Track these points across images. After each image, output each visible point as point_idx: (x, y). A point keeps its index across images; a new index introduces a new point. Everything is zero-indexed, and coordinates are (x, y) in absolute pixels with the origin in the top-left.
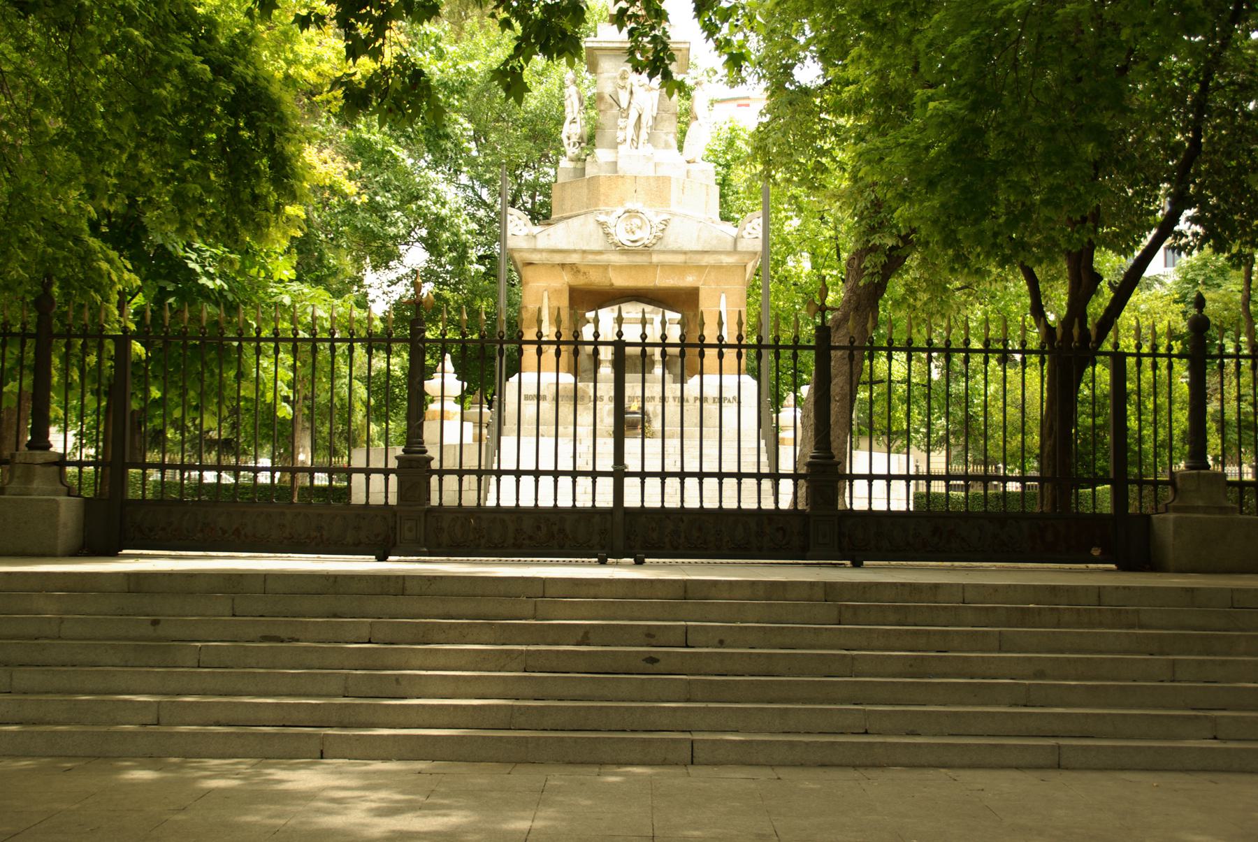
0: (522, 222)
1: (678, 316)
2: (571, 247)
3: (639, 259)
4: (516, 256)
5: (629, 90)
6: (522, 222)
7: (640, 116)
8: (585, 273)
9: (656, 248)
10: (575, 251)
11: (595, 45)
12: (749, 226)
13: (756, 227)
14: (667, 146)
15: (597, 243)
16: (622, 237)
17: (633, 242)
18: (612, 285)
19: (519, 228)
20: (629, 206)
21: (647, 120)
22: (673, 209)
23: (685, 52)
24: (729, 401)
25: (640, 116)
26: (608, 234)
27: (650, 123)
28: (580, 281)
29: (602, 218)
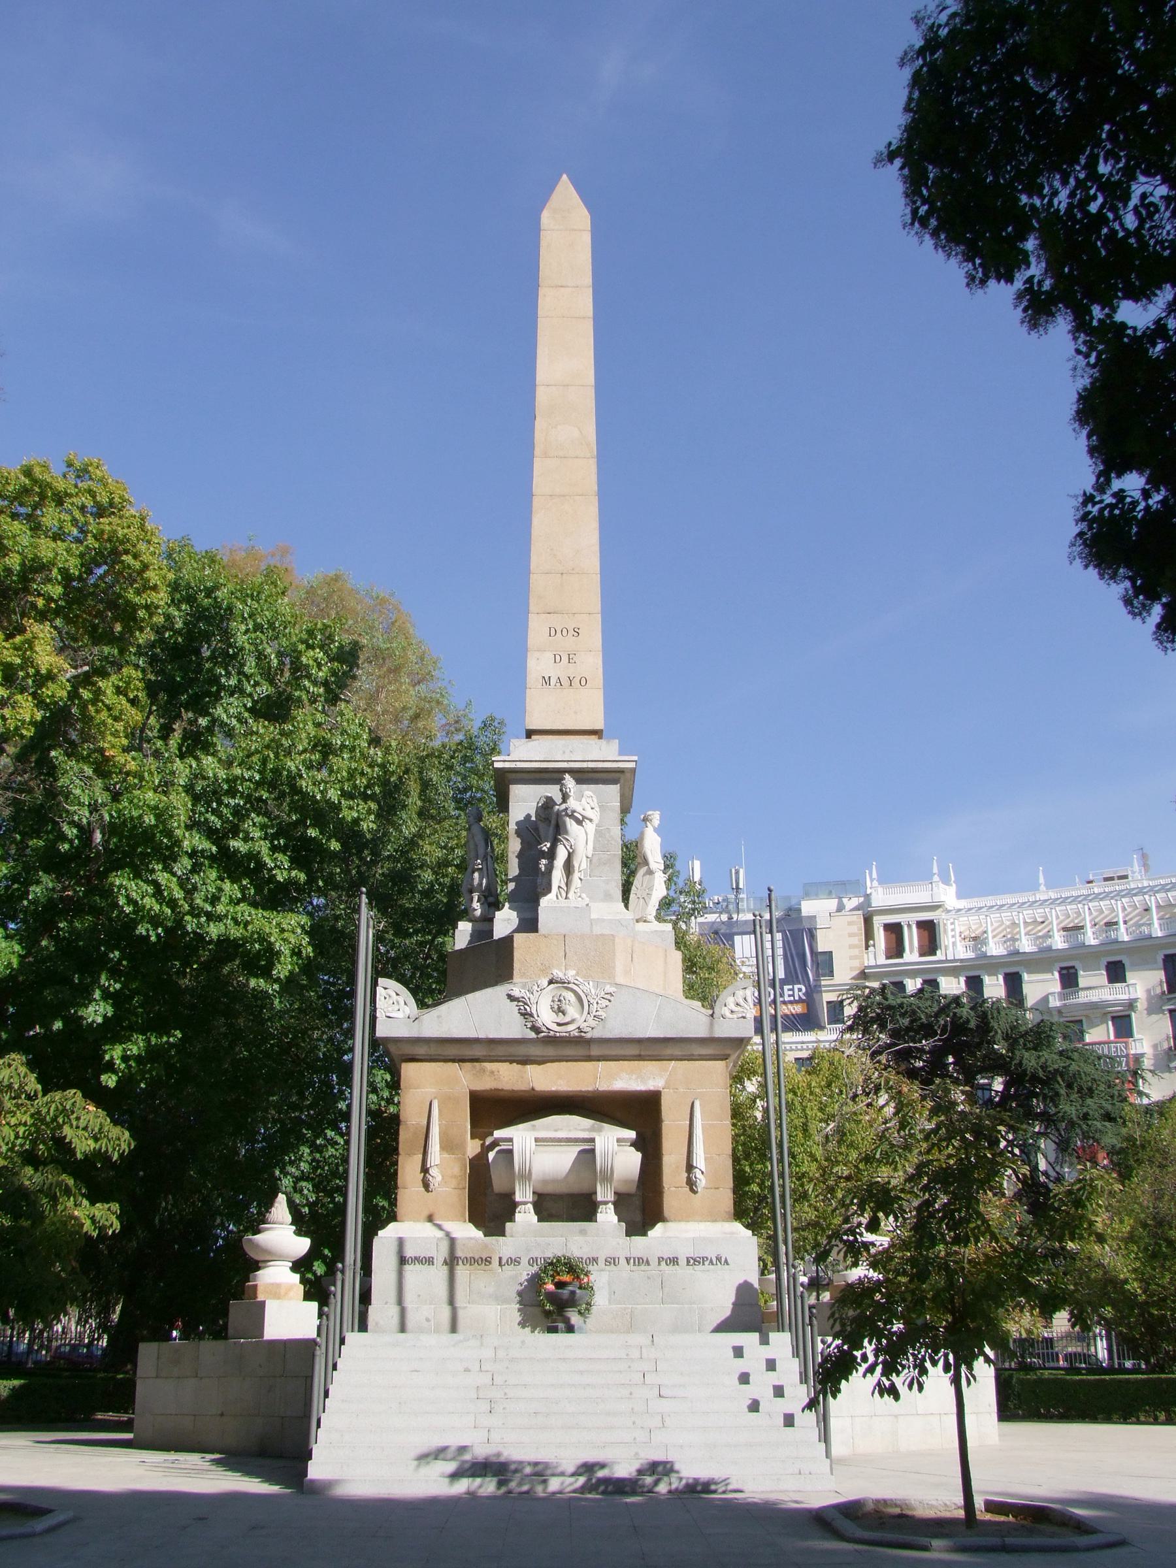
0: (401, 1000)
1: (632, 1134)
2: (472, 1034)
3: (569, 1051)
4: (392, 1049)
5: (553, 822)
6: (401, 1000)
7: (570, 856)
8: (492, 1072)
9: (596, 1034)
10: (477, 1041)
11: (507, 765)
12: (731, 1001)
13: (741, 1002)
14: (608, 897)
15: (512, 1027)
16: (546, 1018)
17: (559, 1024)
18: (533, 1089)
19: (396, 1007)
20: (558, 973)
21: (580, 863)
22: (620, 979)
23: (628, 775)
24: (711, 1262)
25: (570, 856)
26: (526, 1015)
27: (584, 866)
28: (485, 1084)
29: (516, 992)
